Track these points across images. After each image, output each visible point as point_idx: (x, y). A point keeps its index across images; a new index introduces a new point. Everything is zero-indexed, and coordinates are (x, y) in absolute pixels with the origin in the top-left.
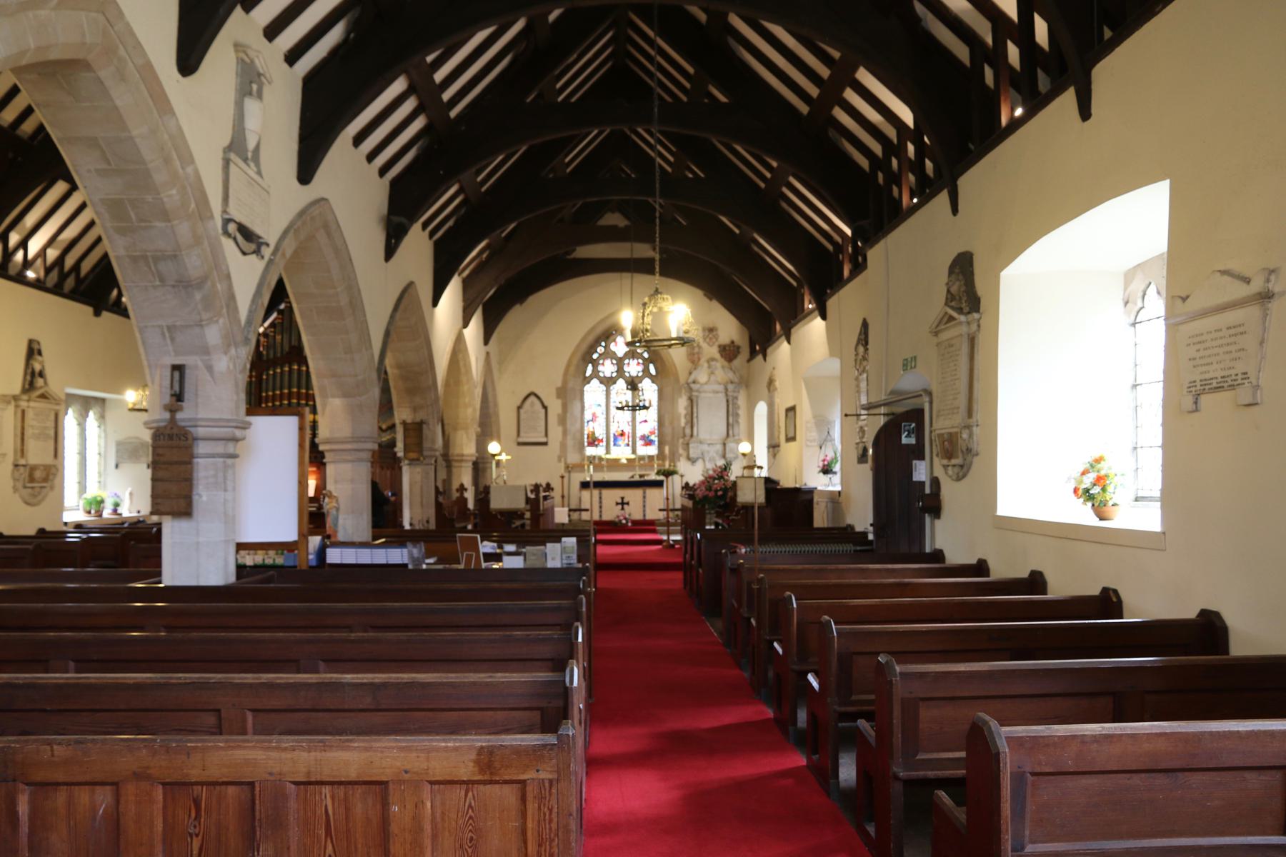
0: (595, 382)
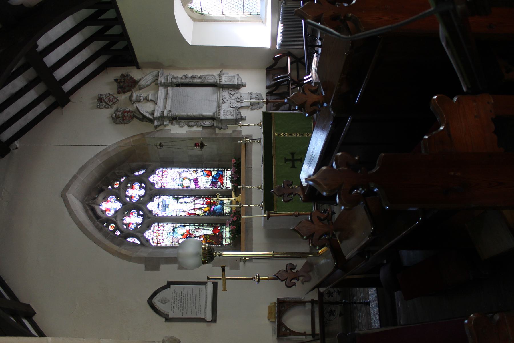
0: (148, 234)
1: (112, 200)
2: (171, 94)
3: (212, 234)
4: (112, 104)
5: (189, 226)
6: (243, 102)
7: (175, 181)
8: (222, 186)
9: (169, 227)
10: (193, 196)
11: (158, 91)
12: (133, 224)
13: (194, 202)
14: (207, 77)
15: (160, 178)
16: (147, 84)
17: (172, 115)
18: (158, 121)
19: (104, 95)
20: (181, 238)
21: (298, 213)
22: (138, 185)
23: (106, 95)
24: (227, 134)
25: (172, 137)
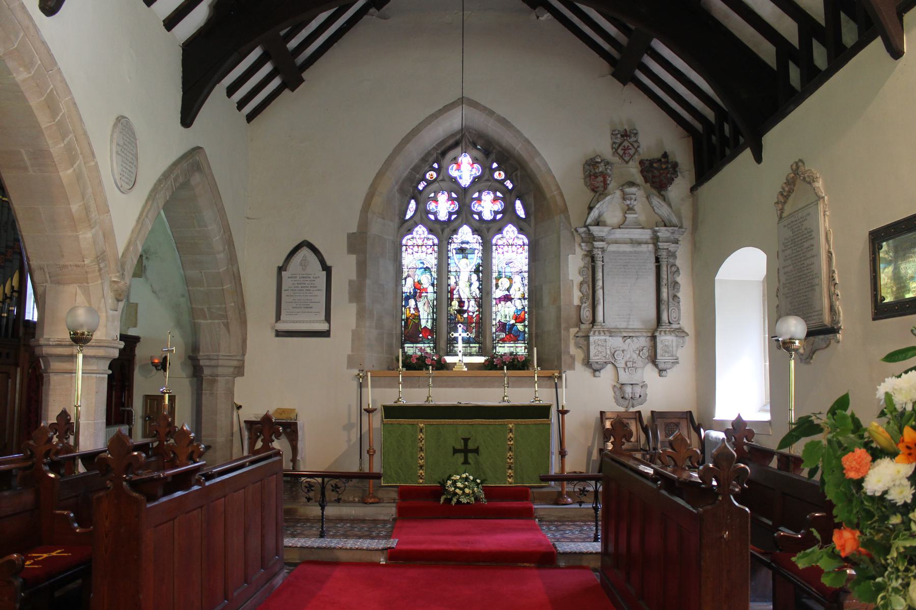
1: (474, 170)
2: (641, 249)
3: (421, 326)
4: (619, 154)
5: (433, 291)
6: (625, 372)
7: (506, 266)
8: (498, 341)
9: (431, 260)
10: (482, 296)
11: (643, 228)
12: (436, 207)
13: (471, 297)
14: (676, 309)
15: (511, 242)
16: (655, 208)
17: (596, 255)
18: (585, 233)
19: (635, 139)
20: (414, 280)
21: (371, 453)
22: (499, 209)
23: (636, 141)
24: (568, 346)
25: (562, 258)
